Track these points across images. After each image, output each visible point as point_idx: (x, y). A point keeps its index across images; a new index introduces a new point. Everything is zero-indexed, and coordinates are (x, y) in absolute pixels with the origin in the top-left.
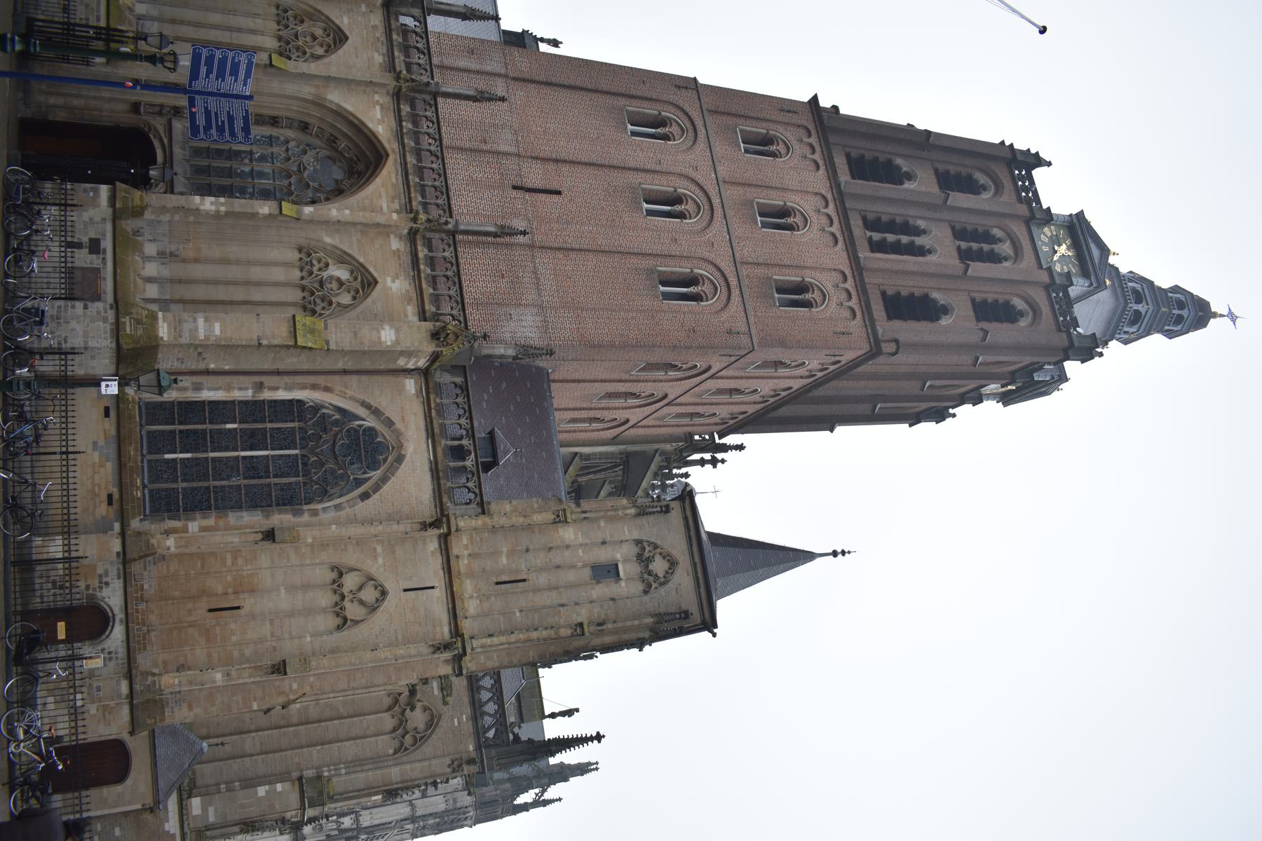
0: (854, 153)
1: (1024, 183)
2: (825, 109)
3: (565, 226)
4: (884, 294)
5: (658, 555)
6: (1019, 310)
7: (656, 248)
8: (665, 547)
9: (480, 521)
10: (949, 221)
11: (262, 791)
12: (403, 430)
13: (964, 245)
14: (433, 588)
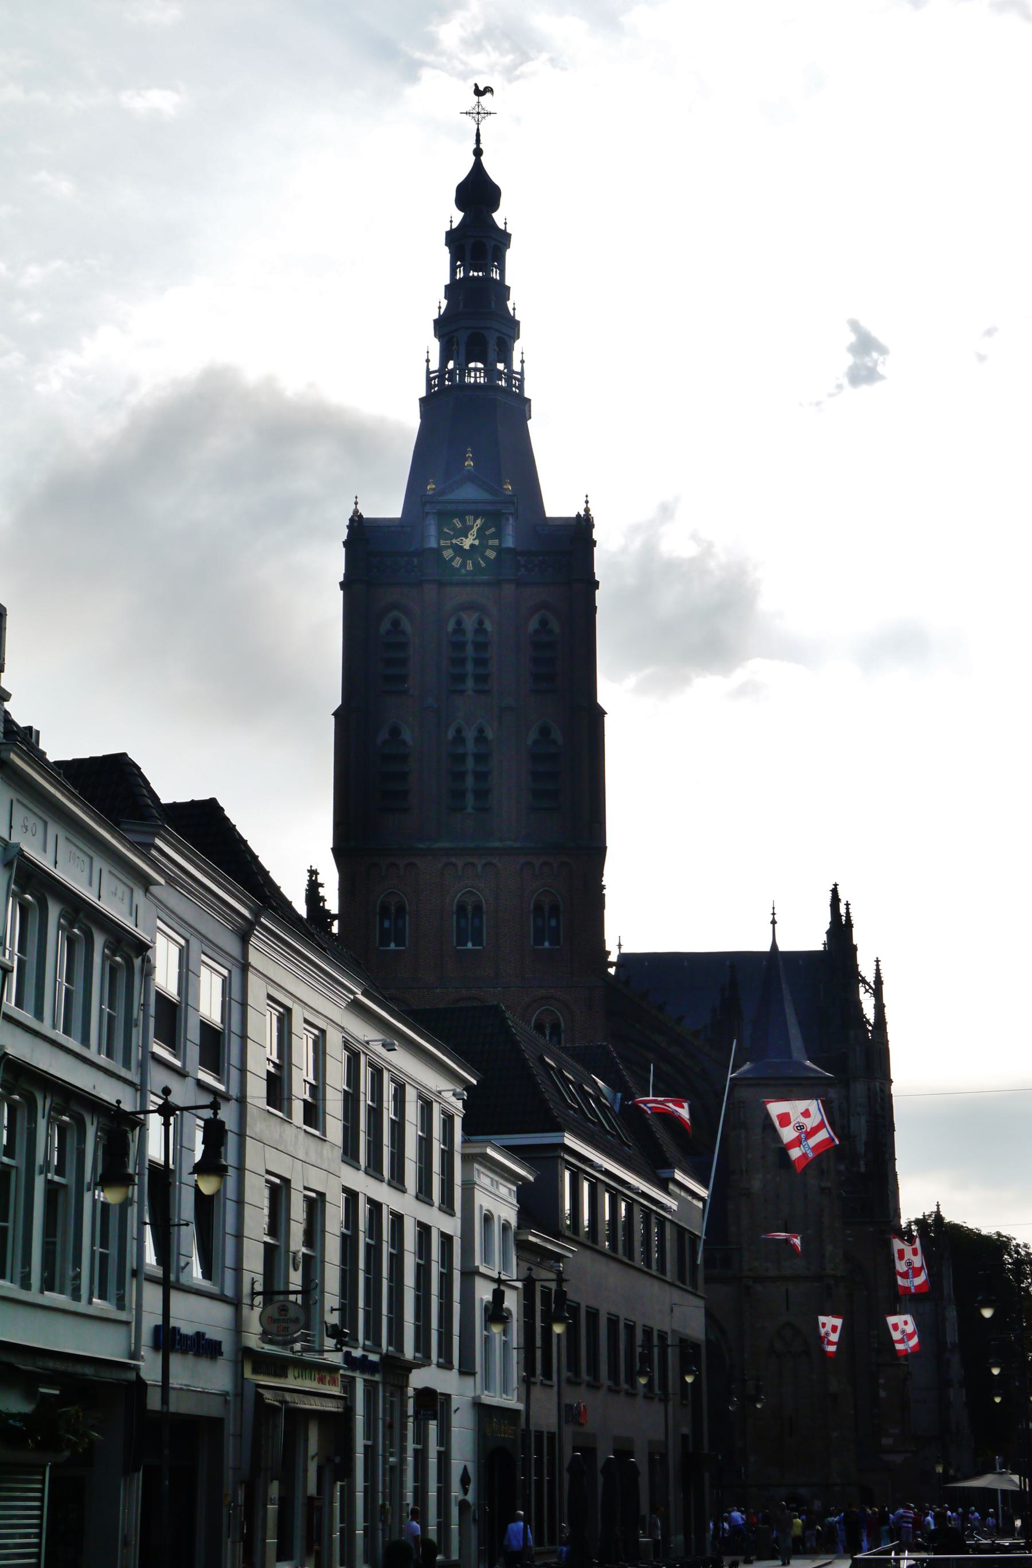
11: (882, 1394)
14: (787, 1290)
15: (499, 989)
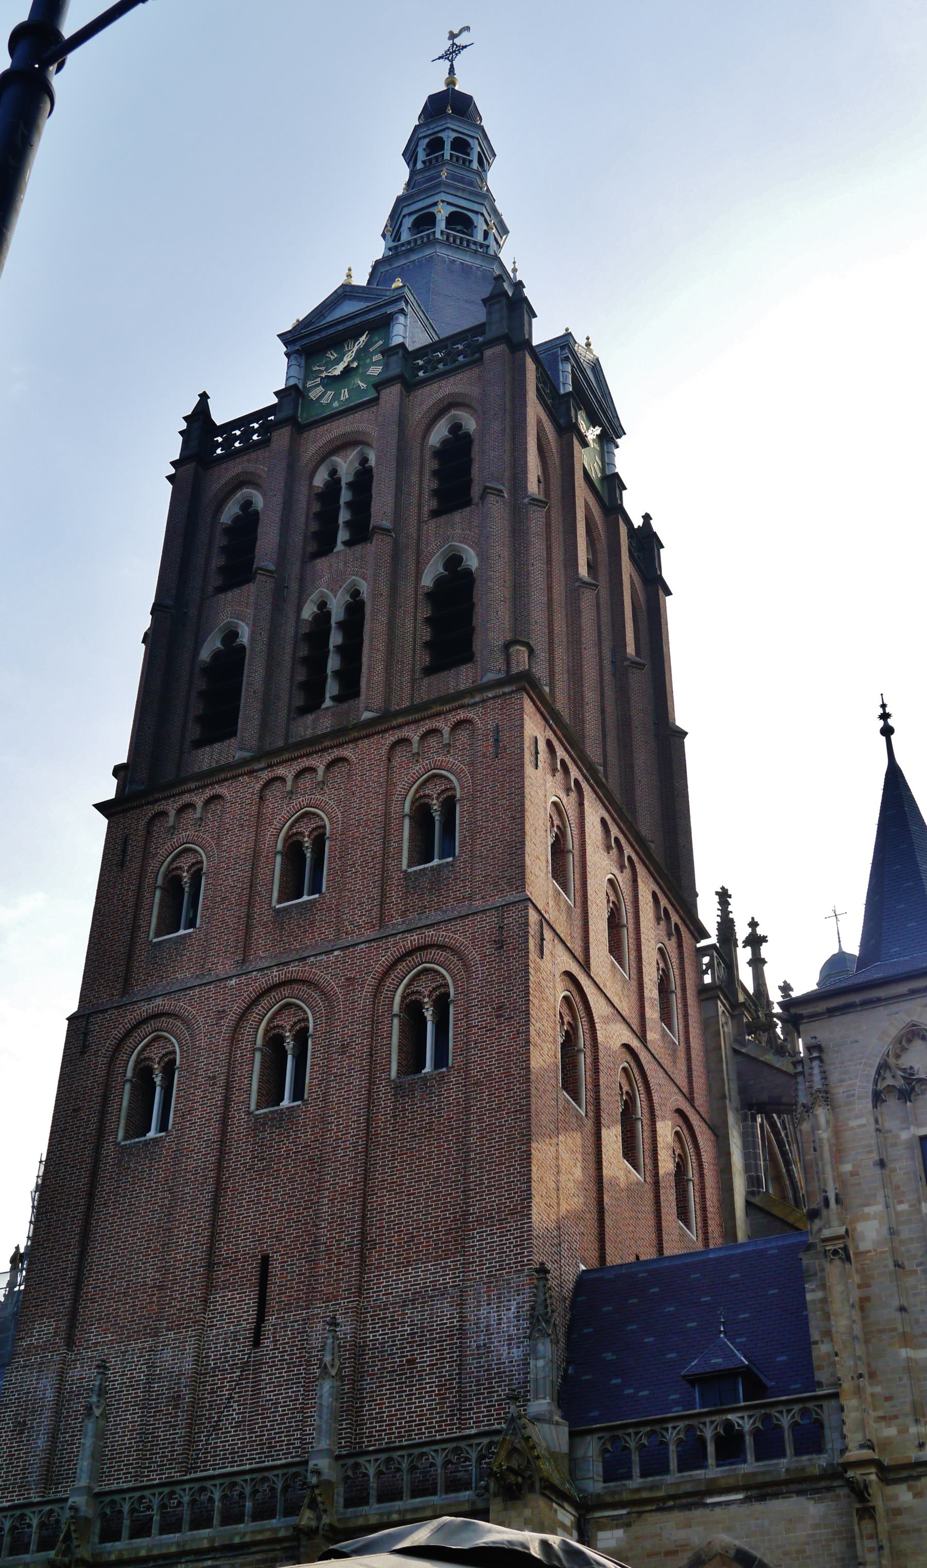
0: (194, 732)
1: (236, 438)
2: (120, 789)
3: (322, 1247)
4: (429, 671)
5: (900, 1062)
6: (450, 431)
7: (358, 1081)
8: (884, 1050)
9: (850, 1402)
10: (304, 563)
12: (689, 1554)
13: (343, 535)
15: (336, 953)
